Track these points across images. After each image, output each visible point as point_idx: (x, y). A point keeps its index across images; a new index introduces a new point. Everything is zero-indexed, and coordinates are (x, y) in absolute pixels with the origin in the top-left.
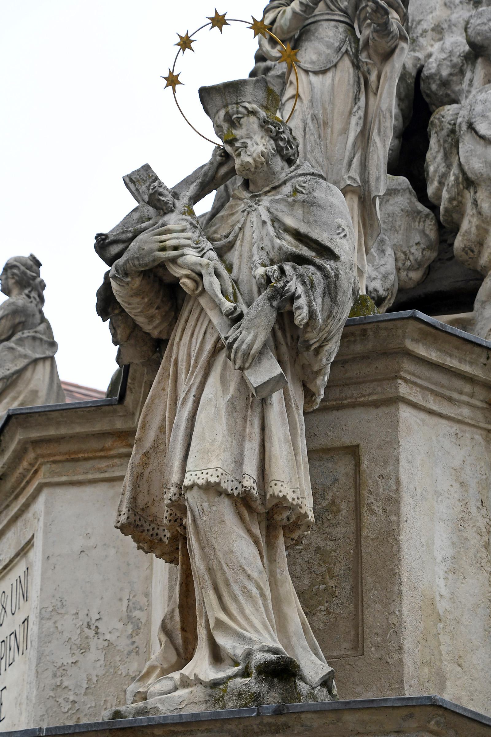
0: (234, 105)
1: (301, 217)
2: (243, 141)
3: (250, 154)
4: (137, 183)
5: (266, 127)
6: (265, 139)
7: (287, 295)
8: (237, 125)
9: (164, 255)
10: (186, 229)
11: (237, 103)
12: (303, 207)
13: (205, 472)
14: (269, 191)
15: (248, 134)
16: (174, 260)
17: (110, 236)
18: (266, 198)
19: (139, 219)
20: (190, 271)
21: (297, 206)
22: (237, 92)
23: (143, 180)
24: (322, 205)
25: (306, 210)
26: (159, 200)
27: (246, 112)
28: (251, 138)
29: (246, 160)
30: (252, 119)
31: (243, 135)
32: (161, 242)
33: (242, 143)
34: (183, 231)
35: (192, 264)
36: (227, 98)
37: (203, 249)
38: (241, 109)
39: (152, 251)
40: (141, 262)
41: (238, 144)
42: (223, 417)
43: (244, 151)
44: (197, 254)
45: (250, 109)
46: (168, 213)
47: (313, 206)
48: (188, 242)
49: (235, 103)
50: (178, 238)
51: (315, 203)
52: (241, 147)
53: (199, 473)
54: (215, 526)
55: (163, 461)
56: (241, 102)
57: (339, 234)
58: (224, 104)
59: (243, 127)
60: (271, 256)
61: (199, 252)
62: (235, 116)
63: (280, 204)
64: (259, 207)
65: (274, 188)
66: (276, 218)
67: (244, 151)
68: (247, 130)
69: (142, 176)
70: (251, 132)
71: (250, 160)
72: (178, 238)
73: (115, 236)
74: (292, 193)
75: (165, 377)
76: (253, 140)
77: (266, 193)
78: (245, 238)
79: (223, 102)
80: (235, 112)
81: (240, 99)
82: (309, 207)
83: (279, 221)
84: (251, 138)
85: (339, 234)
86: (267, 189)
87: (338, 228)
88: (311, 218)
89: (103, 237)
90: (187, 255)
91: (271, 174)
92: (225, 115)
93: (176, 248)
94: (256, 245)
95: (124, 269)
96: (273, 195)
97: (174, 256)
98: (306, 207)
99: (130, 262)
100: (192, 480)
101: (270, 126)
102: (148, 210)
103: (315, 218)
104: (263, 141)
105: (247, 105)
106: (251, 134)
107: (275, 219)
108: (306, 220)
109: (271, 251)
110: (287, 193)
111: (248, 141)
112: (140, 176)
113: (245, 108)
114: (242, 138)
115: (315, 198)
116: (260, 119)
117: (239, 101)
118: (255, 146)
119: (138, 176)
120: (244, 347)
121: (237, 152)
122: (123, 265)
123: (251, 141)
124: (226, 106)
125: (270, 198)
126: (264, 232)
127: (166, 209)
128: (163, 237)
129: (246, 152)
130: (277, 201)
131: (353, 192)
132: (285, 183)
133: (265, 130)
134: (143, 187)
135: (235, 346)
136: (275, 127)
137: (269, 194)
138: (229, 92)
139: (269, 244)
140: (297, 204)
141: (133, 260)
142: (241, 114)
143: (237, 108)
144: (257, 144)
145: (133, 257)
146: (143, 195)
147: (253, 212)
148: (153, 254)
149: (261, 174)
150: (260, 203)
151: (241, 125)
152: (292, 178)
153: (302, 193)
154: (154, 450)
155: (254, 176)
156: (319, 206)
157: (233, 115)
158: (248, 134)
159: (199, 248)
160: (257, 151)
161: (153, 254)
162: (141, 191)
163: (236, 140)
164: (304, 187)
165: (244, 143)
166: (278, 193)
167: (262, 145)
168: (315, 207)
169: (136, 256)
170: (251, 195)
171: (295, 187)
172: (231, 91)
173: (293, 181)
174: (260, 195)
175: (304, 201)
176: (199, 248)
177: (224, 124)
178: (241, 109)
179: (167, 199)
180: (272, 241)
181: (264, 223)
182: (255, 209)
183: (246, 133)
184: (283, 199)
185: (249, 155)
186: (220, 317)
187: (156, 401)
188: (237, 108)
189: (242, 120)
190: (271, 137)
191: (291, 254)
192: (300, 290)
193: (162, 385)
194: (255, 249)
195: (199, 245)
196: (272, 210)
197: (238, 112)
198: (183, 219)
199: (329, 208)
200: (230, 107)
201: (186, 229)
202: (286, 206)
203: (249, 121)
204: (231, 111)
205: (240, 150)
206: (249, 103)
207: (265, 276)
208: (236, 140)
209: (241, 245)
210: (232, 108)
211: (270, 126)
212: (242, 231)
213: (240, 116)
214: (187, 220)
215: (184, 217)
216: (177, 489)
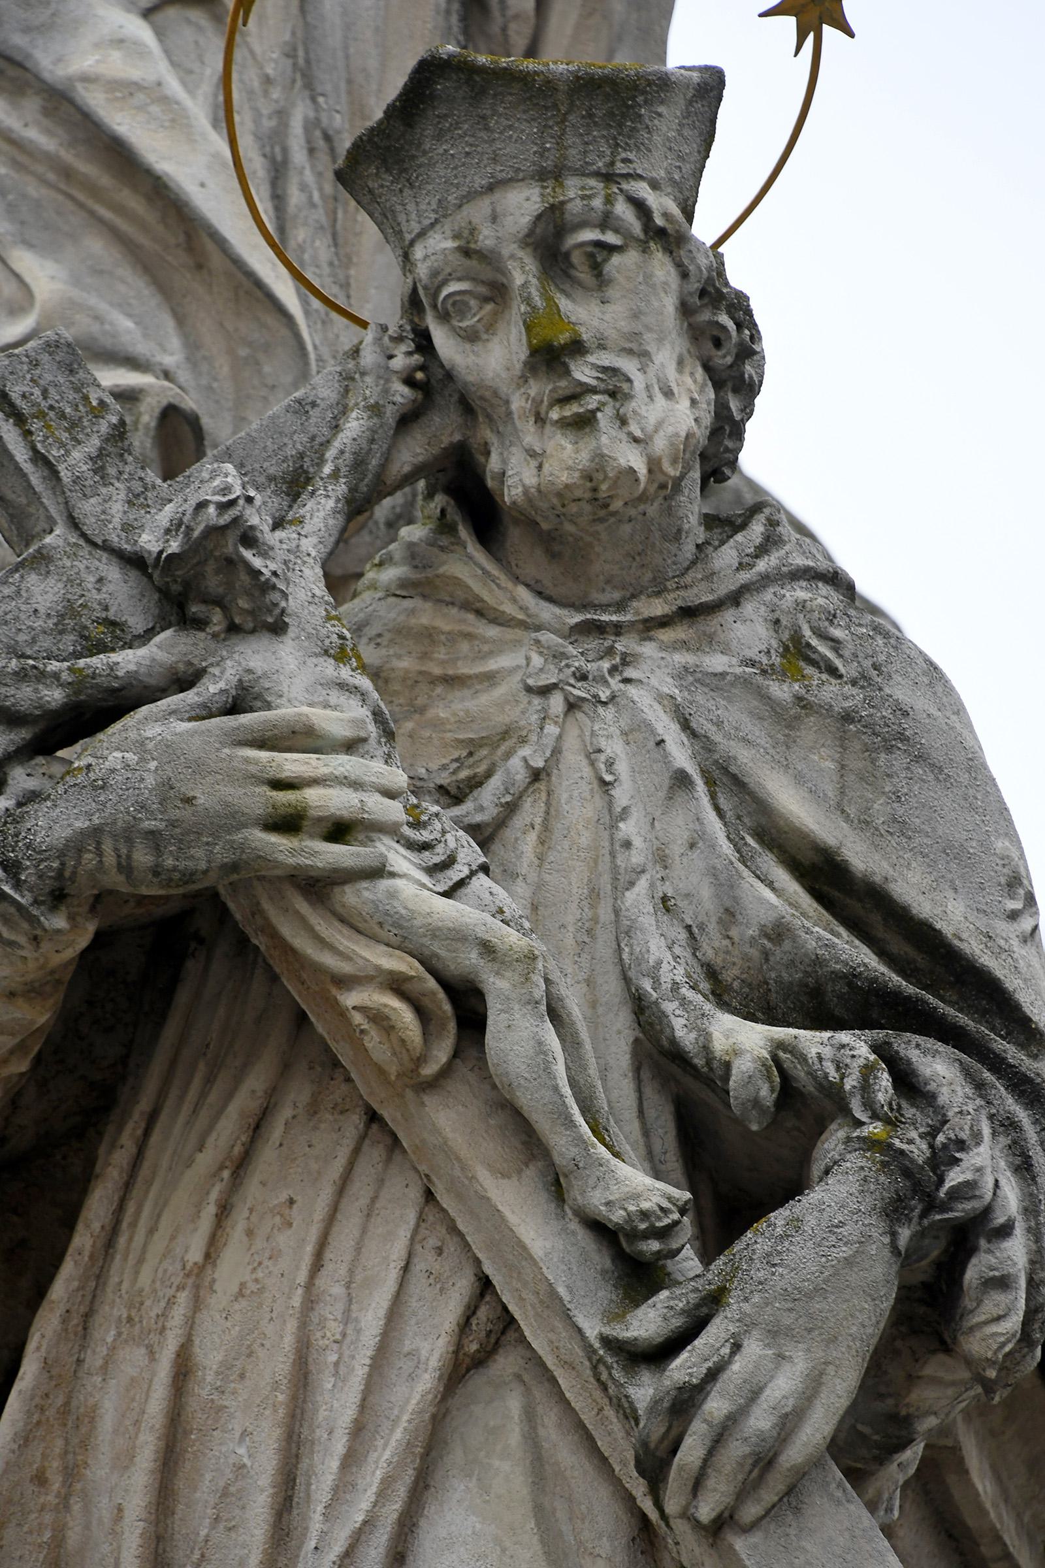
0: (592, 182)
1: (831, 791)
2: (606, 359)
3: (638, 433)
5: (705, 316)
6: (692, 374)
8: (583, 274)
9: (293, 852)
10: (364, 740)
11: (608, 178)
12: (843, 741)
14: (664, 622)
15: (636, 335)
18: (648, 649)
22: (620, 125)
24: (938, 756)
25: (856, 763)
26: (232, 563)
27: (636, 227)
28: (643, 356)
29: (623, 462)
30: (662, 268)
31: (611, 333)
32: (279, 785)
33: (605, 369)
34: (351, 746)
35: (435, 933)
36: (570, 139)
37: (449, 862)
38: (622, 209)
39: (233, 820)
41: (583, 373)
43: (609, 410)
45: (659, 221)
46: (253, 631)
47: (889, 749)
48: (394, 811)
49: (597, 174)
50: (356, 785)
52: (594, 391)
56: (628, 176)
57: (1013, 916)
59: (612, 292)
60: (708, 952)
61: (434, 870)
63: (729, 700)
64: (632, 691)
65: (689, 613)
66: (725, 770)
67: (609, 410)
68: (636, 315)
70: (649, 329)
71: (634, 459)
72: (356, 785)
76: (652, 370)
77: (649, 627)
78: (558, 827)
80: (596, 217)
81: (626, 161)
83: (739, 784)
84: (643, 356)
85: (1013, 916)
86: (658, 608)
88: (880, 809)
90: (393, 875)
91: (664, 538)
92: (539, 217)
94: (643, 884)
96: (684, 645)
97: (335, 870)
101: (724, 319)
104: (689, 381)
106: (647, 336)
107: (717, 774)
108: (852, 811)
109: (712, 927)
110: (752, 654)
111: (629, 366)
113: (640, 207)
114: (602, 347)
115: (906, 714)
116: (684, 275)
117: (621, 168)
118: (659, 398)
121: (574, 409)
123: (642, 369)
125: (681, 658)
126: (677, 828)
127: (252, 613)
128: (292, 764)
129: (623, 422)
130: (717, 682)
132: (735, 599)
133: (690, 325)
136: (739, 326)
137: (666, 635)
138: (591, 116)
139: (706, 892)
142: (616, 231)
143: (609, 200)
144: (668, 394)
147: (600, 710)
148: (238, 837)
149: (627, 528)
150: (630, 673)
152: (766, 580)
153: (833, 671)
155: (600, 527)
156: (920, 758)
158: (636, 335)
159: (425, 847)
160: (670, 430)
161: (238, 837)
164: (836, 644)
166: (709, 642)
167: (687, 403)
168: (899, 761)
172: (599, 113)
173: (768, 595)
174: (618, 629)
175: (847, 717)
176: (425, 847)
177: (520, 254)
179: (273, 566)
180: (725, 885)
181: (681, 780)
182: (613, 698)
184: (745, 682)
185: (636, 440)
189: (616, 259)
190: (707, 368)
194: (638, 898)
195: (425, 836)
196: (701, 723)
197: (606, 222)
198: (342, 686)
199: (964, 778)
200: (572, 188)
201: (364, 740)
203: (648, 277)
204: (575, 207)
205: (593, 401)
206: (655, 185)
208: (577, 347)
209: (541, 858)
211: (724, 319)
212: (542, 786)
213: (611, 238)
214: (363, 696)
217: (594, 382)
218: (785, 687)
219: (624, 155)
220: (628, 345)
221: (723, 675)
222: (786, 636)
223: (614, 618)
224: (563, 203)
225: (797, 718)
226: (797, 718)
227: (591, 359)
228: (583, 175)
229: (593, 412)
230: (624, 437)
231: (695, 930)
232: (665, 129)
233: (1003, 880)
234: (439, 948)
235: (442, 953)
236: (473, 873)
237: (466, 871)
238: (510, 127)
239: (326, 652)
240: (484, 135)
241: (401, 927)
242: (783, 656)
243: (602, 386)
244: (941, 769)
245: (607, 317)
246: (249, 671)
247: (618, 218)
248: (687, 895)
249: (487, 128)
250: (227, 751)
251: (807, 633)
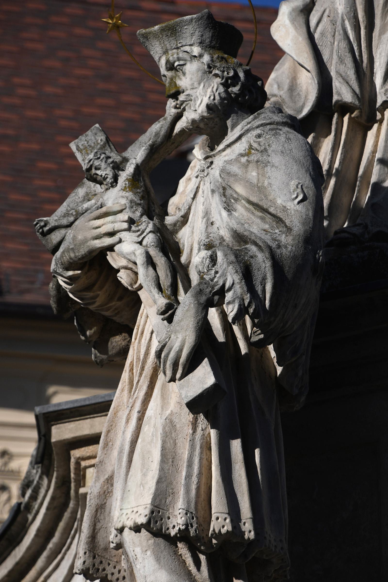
16: (111, 248)
19: (84, 197)
22: (175, 35)
25: (261, 172)
33: (187, 95)
40: (77, 254)
47: (267, 166)
49: (175, 49)
51: (269, 162)
52: (186, 101)
56: (182, 46)
69: (90, 142)
79: (162, 48)
80: (176, 59)
82: (263, 168)
93: (111, 234)
95: (62, 263)
105: (187, 48)
107: (226, 186)
112: (88, 142)
114: (187, 90)
117: (179, 45)
119: (86, 143)
120: (172, 355)
124: (166, 52)
140: (251, 165)
141: (69, 252)
143: (178, 54)
145: (68, 248)
148: (88, 244)
157: (175, 62)
159: (138, 231)
161: (88, 244)
169: (71, 247)
175: (257, 161)
176: (138, 231)
188: (178, 54)
189: (184, 67)
204: (171, 59)
213: (182, 62)
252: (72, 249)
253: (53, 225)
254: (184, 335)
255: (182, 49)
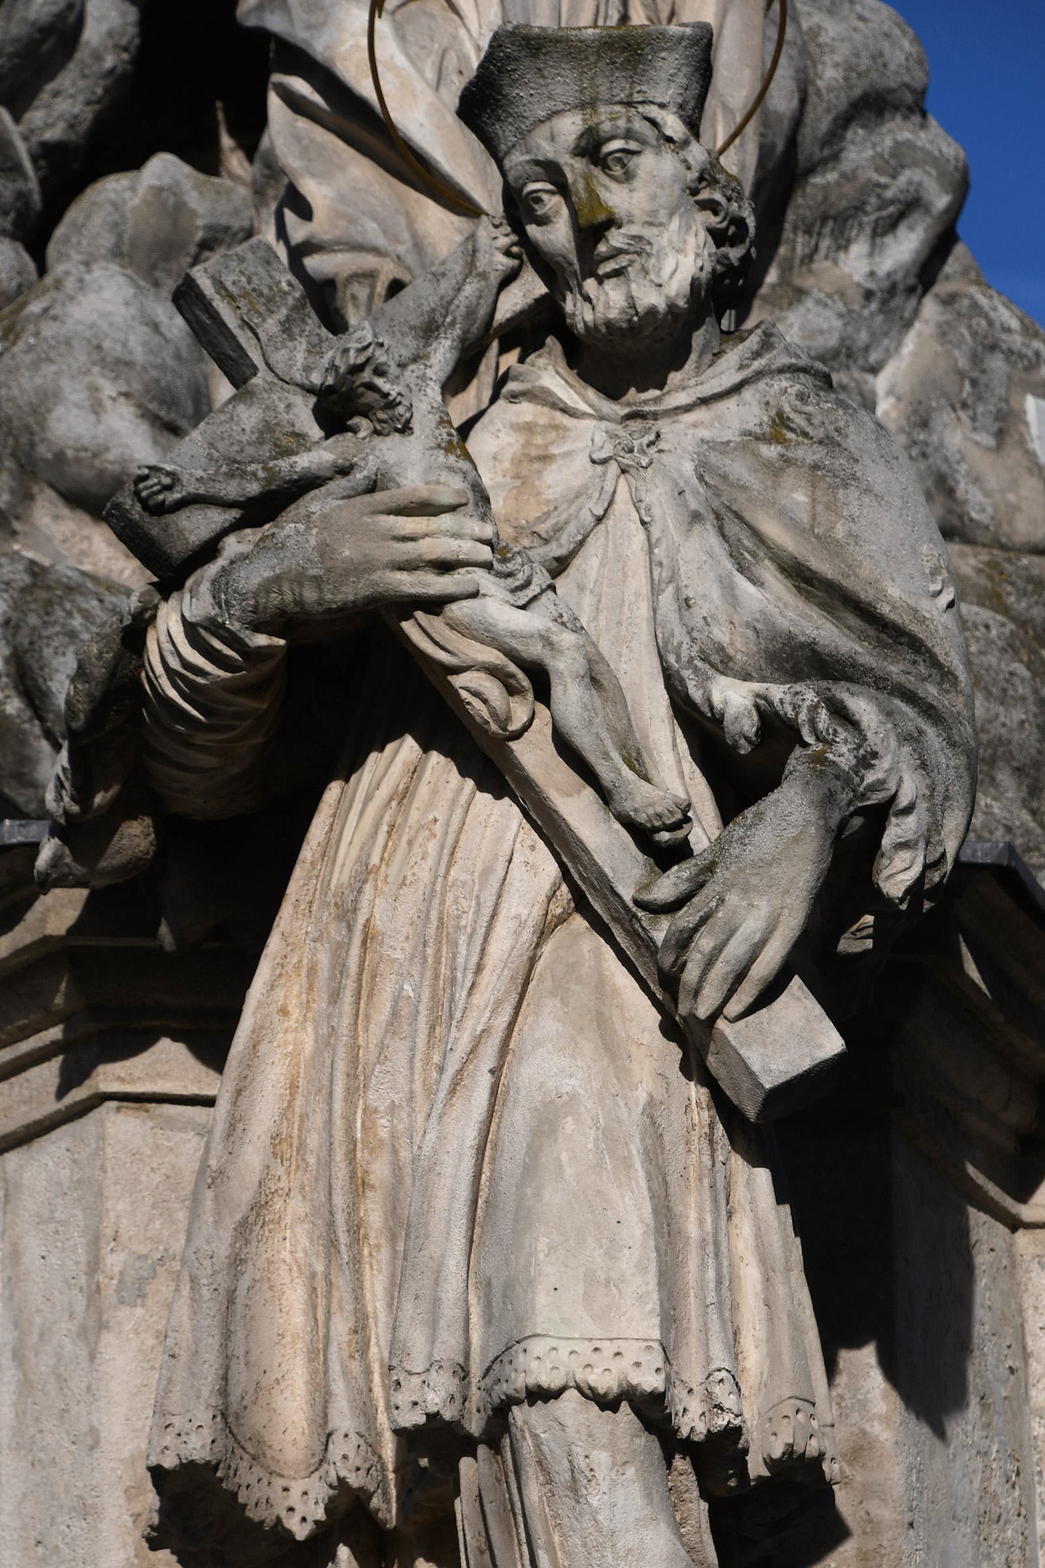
0: (618, 108)
2: (634, 230)
4: (242, 303)
7: (875, 798)
13: (609, 1348)
16: (435, 605)
17: (185, 478)
19: (261, 433)
20: (501, 656)
21: (790, 477)
23: (261, 294)
26: (371, 387)
31: (637, 212)
33: (633, 237)
35: (513, 634)
36: (600, 80)
37: (527, 584)
38: (639, 125)
40: (329, 596)
42: (638, 1166)
44: (509, 597)
47: (846, 486)
49: (620, 103)
50: (456, 536)
51: (854, 477)
52: (626, 252)
53: (585, 1348)
54: (628, 1531)
55: (279, 1252)
58: (586, 98)
59: (637, 183)
62: (616, 144)
67: (637, 266)
69: (254, 279)
73: (200, 480)
74: (767, 429)
75: (289, 968)
80: (621, 131)
82: (833, 488)
87: (932, 574)
89: (166, 481)
92: (581, 136)
93: (444, 567)
95: (256, 606)
98: (823, 485)
99: (286, 588)
100: (562, 1371)
102: (289, 406)
103: (854, 528)
105: (654, 112)
107: (723, 511)
112: (249, 281)
114: (631, 222)
117: (637, 97)
119: (243, 279)
120: (736, 949)
122: (256, 595)
124: (587, 104)
129: (645, 271)
131: (175, 223)
134: (270, 321)
135: (704, 943)
140: (791, 470)
141: (301, 584)
142: (637, 140)
146: (268, 350)
151: (628, 177)
154: (258, 1215)
156: (868, 490)
157: (613, 138)
159: (510, 575)
161: (375, 576)
162: (261, 335)
163: (612, 222)
165: (638, 238)
168: (853, 493)
169: (311, 572)
170: (626, 411)
171: (780, 414)
173: (762, 385)
174: (655, 416)
175: (815, 467)
176: (510, 575)
178: (639, 125)
182: (651, 463)
183: (647, 206)
186: (605, 827)
187: (263, 1048)
188: (629, 120)
189: (635, 160)
191: (803, 646)
192: (909, 788)
193: (280, 994)
195: (510, 567)
198: (450, 469)
200: (604, 110)
202: (756, 471)
204: (606, 127)
207: (754, 712)
208: (612, 222)
210: (608, 118)
213: (633, 145)
215: (452, 459)
216: (456, 1381)
217: (625, 247)
218: (772, 448)
219: (638, 88)
220: (649, 219)
221: (728, 443)
222: (773, 412)
223: (653, 408)
224: (598, 124)
225: (781, 469)
226: (781, 469)
227: (622, 231)
228: (611, 104)
229: (625, 268)
230: (648, 284)
231: (709, 620)
232: (666, 67)
233: (927, 571)
234: (514, 644)
235: (519, 647)
236: (543, 591)
237: (538, 590)
238: (558, 74)
239: (439, 446)
240: (541, 81)
241: (489, 631)
242: (771, 427)
243: (632, 249)
244: (882, 499)
245: (634, 201)
246: (385, 462)
247: (637, 132)
248: (704, 596)
249: (543, 77)
250: (365, 519)
251: (787, 409)
252: (315, 577)
253: (191, 490)
254: (777, 902)
255: (641, 109)
